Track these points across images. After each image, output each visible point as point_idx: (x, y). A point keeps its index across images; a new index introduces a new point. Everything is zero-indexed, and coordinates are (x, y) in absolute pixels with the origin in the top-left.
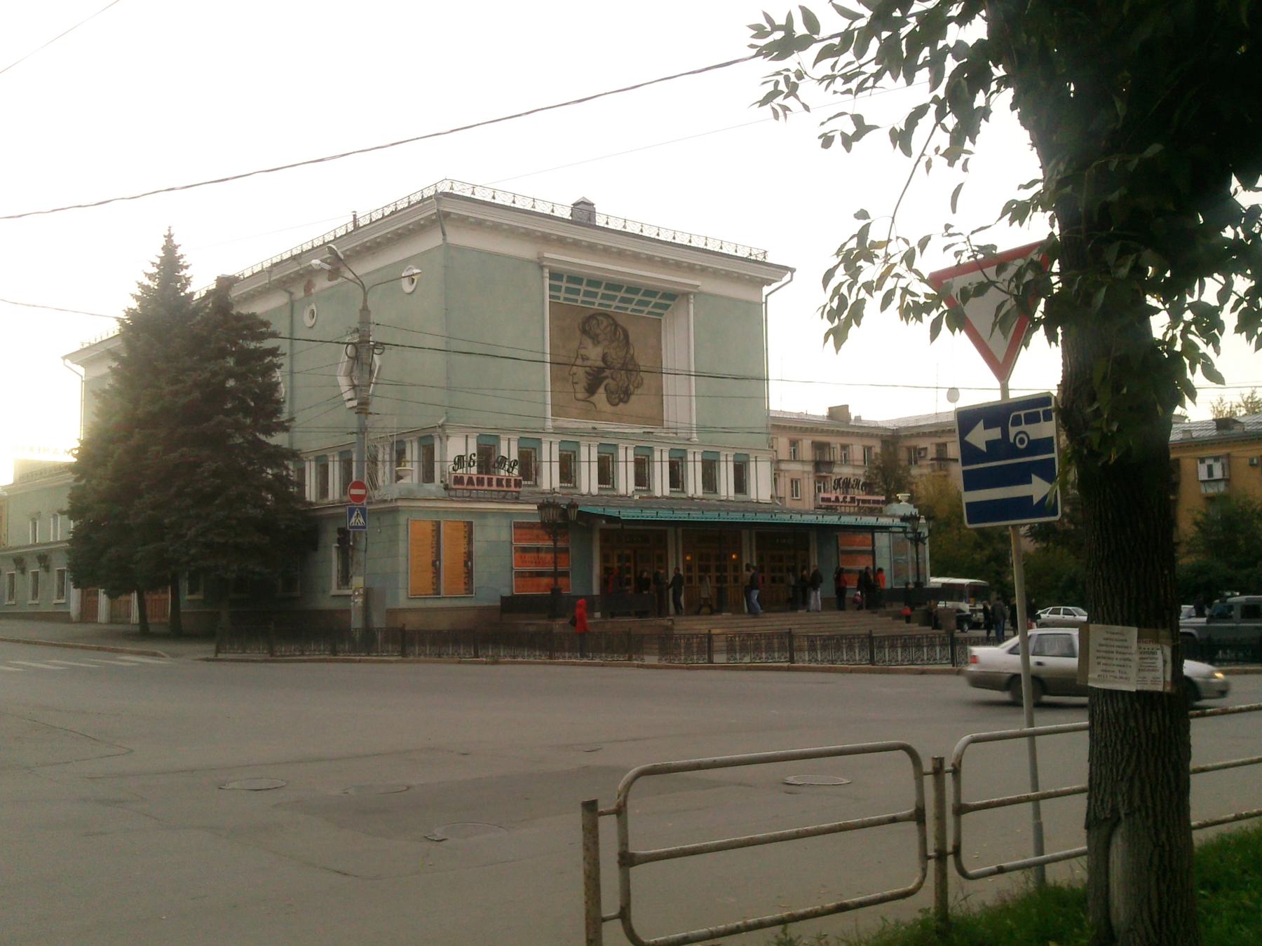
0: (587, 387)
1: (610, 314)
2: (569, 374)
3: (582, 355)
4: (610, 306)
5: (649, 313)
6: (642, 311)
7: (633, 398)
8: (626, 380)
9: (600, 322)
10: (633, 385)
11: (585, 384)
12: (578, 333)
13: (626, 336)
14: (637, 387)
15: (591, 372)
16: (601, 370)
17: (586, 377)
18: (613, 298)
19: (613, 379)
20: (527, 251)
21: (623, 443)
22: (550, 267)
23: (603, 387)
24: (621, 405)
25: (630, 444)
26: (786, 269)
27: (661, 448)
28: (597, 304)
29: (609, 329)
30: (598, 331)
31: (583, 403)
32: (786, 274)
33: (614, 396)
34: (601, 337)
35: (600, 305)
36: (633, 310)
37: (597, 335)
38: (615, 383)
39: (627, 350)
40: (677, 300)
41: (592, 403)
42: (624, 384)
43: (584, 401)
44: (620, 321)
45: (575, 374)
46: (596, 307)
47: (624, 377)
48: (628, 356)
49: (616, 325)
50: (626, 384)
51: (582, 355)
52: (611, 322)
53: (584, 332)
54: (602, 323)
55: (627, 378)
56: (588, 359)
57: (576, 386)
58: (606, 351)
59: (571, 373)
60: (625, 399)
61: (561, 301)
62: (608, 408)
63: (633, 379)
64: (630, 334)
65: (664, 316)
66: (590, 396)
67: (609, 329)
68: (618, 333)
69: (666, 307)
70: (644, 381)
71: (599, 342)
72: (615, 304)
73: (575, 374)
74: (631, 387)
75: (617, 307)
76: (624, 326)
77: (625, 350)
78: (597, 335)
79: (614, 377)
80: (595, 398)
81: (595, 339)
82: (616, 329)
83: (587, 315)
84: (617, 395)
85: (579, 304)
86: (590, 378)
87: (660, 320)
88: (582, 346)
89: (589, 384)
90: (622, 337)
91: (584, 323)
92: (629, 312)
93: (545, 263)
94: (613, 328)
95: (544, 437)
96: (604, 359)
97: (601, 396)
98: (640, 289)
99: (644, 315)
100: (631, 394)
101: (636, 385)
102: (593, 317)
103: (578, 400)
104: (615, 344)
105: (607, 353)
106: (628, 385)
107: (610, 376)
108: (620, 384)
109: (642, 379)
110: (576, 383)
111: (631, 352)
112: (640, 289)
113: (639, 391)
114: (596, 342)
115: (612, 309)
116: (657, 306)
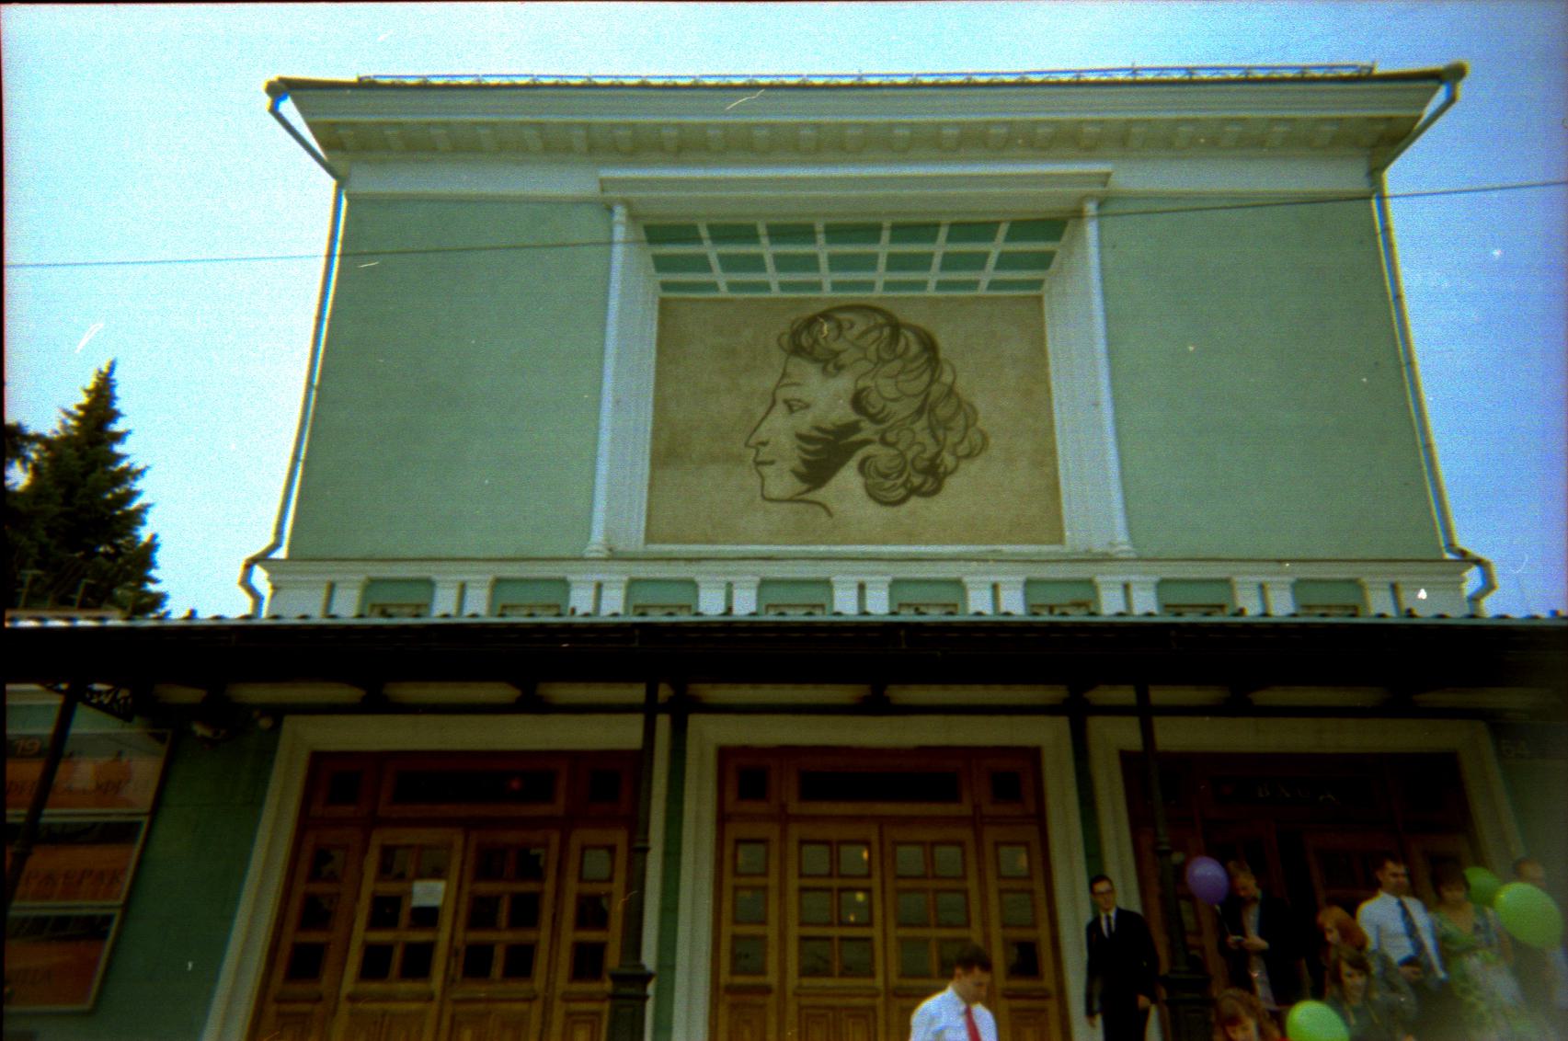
0: (803, 469)
1: (876, 304)
2: (746, 445)
3: (786, 402)
4: (870, 286)
5: (994, 285)
6: (973, 285)
7: (952, 483)
8: (928, 441)
9: (846, 325)
10: (954, 453)
11: (796, 463)
12: (778, 357)
13: (929, 345)
14: (969, 456)
15: (815, 434)
16: (853, 428)
17: (800, 448)
18: (869, 262)
19: (884, 441)
20: (574, 182)
21: (846, 573)
22: (627, 203)
23: (853, 463)
24: (915, 502)
25: (872, 573)
26: (1435, 77)
27: (993, 579)
28: (827, 285)
29: (875, 334)
30: (837, 346)
31: (786, 506)
32: (1434, 91)
33: (888, 484)
34: (844, 358)
35: (837, 286)
36: (942, 285)
37: (837, 354)
38: (893, 452)
39: (933, 375)
40: (1065, 238)
41: (819, 504)
42: (924, 451)
43: (790, 500)
44: (907, 315)
45: (764, 444)
46: (827, 292)
47: (925, 437)
48: (936, 390)
49: (896, 327)
50: (926, 455)
51: (786, 402)
52: (880, 320)
53: (797, 350)
54: (852, 326)
55: (935, 437)
56: (807, 406)
57: (766, 470)
58: (861, 384)
59: (753, 441)
60: (927, 487)
61: (724, 293)
62: (872, 510)
63: (952, 438)
64: (943, 341)
65: (1046, 286)
66: (808, 491)
67: (875, 334)
68: (902, 343)
69: (1044, 261)
70: (992, 441)
71: (839, 368)
72: (880, 276)
73: (764, 444)
74: (949, 460)
75: (889, 286)
76: (921, 323)
77: (926, 378)
78: (837, 354)
79: (891, 437)
80: (820, 494)
81: (831, 363)
82: (895, 336)
83: (810, 313)
84: (900, 481)
85: (775, 292)
86: (810, 447)
87: (1039, 299)
88: (785, 381)
89: (805, 462)
90: (915, 348)
91: (795, 334)
92: (931, 292)
93: (614, 194)
94: (886, 331)
95: (574, 573)
96: (858, 402)
97: (848, 478)
98: (937, 226)
99: (982, 291)
100: (948, 473)
101: (962, 450)
102: (826, 315)
103: (771, 500)
104: (897, 365)
105: (864, 389)
106: (938, 454)
107: (876, 438)
108: (910, 455)
109: (985, 438)
110: (772, 463)
111: (947, 378)
112: (937, 226)
113: (972, 468)
114: (830, 367)
115: (878, 292)
116: (1006, 261)
